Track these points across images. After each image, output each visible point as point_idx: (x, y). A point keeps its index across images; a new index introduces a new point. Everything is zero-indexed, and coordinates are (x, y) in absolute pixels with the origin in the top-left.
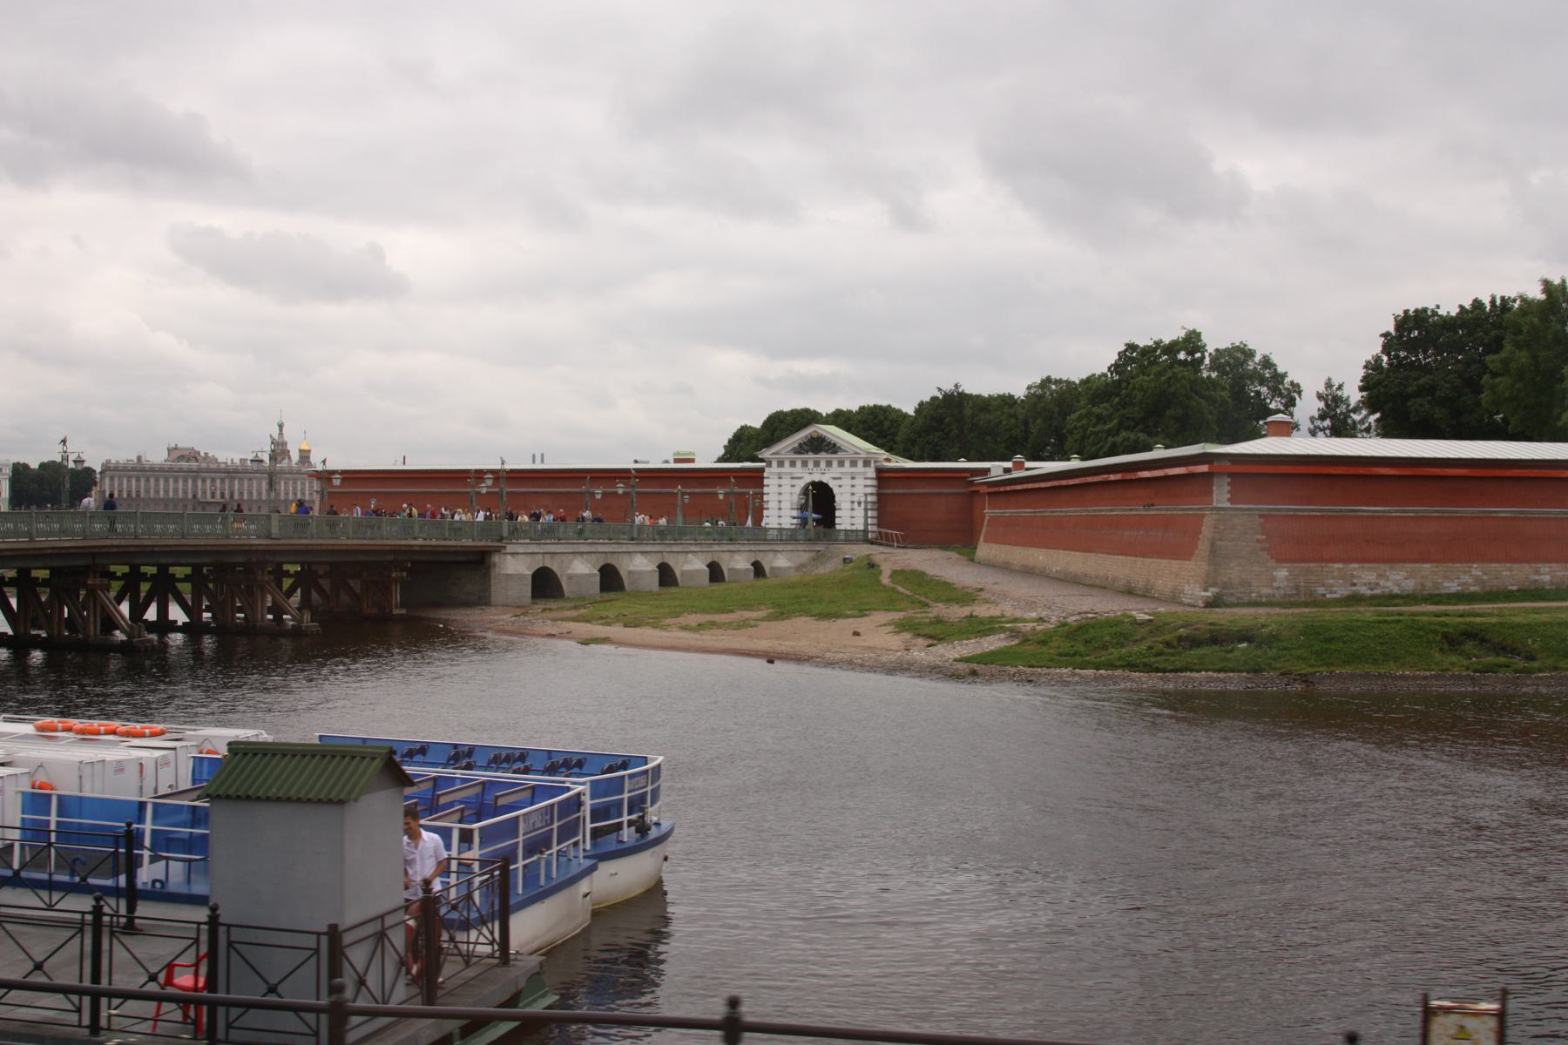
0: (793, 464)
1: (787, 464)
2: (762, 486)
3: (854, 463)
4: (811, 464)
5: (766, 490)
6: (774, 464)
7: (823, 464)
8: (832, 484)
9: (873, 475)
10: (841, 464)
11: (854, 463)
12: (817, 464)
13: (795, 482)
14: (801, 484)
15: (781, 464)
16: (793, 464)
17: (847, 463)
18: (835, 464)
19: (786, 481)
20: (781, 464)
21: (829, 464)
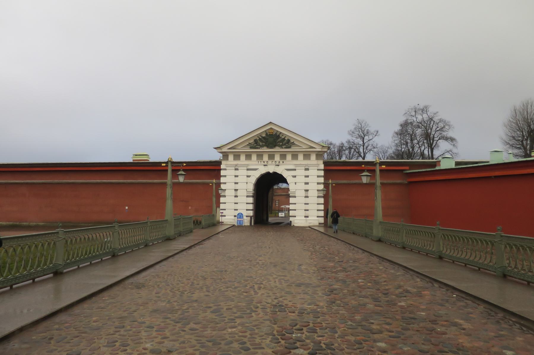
0: (248, 157)
1: (243, 157)
2: (218, 176)
3: (307, 156)
4: (266, 158)
5: (222, 180)
6: (231, 157)
7: (277, 158)
8: (285, 174)
9: (322, 166)
10: (295, 156)
11: (307, 156)
12: (271, 157)
13: (250, 173)
14: (256, 175)
15: (237, 157)
16: (248, 157)
17: (301, 157)
18: (289, 157)
19: (242, 172)
20: (237, 157)
21: (283, 157)
